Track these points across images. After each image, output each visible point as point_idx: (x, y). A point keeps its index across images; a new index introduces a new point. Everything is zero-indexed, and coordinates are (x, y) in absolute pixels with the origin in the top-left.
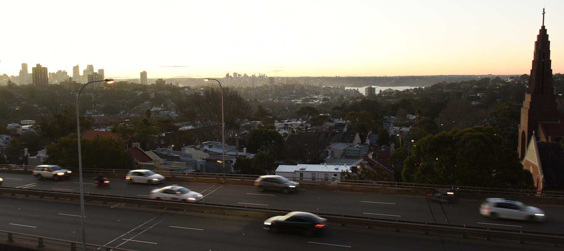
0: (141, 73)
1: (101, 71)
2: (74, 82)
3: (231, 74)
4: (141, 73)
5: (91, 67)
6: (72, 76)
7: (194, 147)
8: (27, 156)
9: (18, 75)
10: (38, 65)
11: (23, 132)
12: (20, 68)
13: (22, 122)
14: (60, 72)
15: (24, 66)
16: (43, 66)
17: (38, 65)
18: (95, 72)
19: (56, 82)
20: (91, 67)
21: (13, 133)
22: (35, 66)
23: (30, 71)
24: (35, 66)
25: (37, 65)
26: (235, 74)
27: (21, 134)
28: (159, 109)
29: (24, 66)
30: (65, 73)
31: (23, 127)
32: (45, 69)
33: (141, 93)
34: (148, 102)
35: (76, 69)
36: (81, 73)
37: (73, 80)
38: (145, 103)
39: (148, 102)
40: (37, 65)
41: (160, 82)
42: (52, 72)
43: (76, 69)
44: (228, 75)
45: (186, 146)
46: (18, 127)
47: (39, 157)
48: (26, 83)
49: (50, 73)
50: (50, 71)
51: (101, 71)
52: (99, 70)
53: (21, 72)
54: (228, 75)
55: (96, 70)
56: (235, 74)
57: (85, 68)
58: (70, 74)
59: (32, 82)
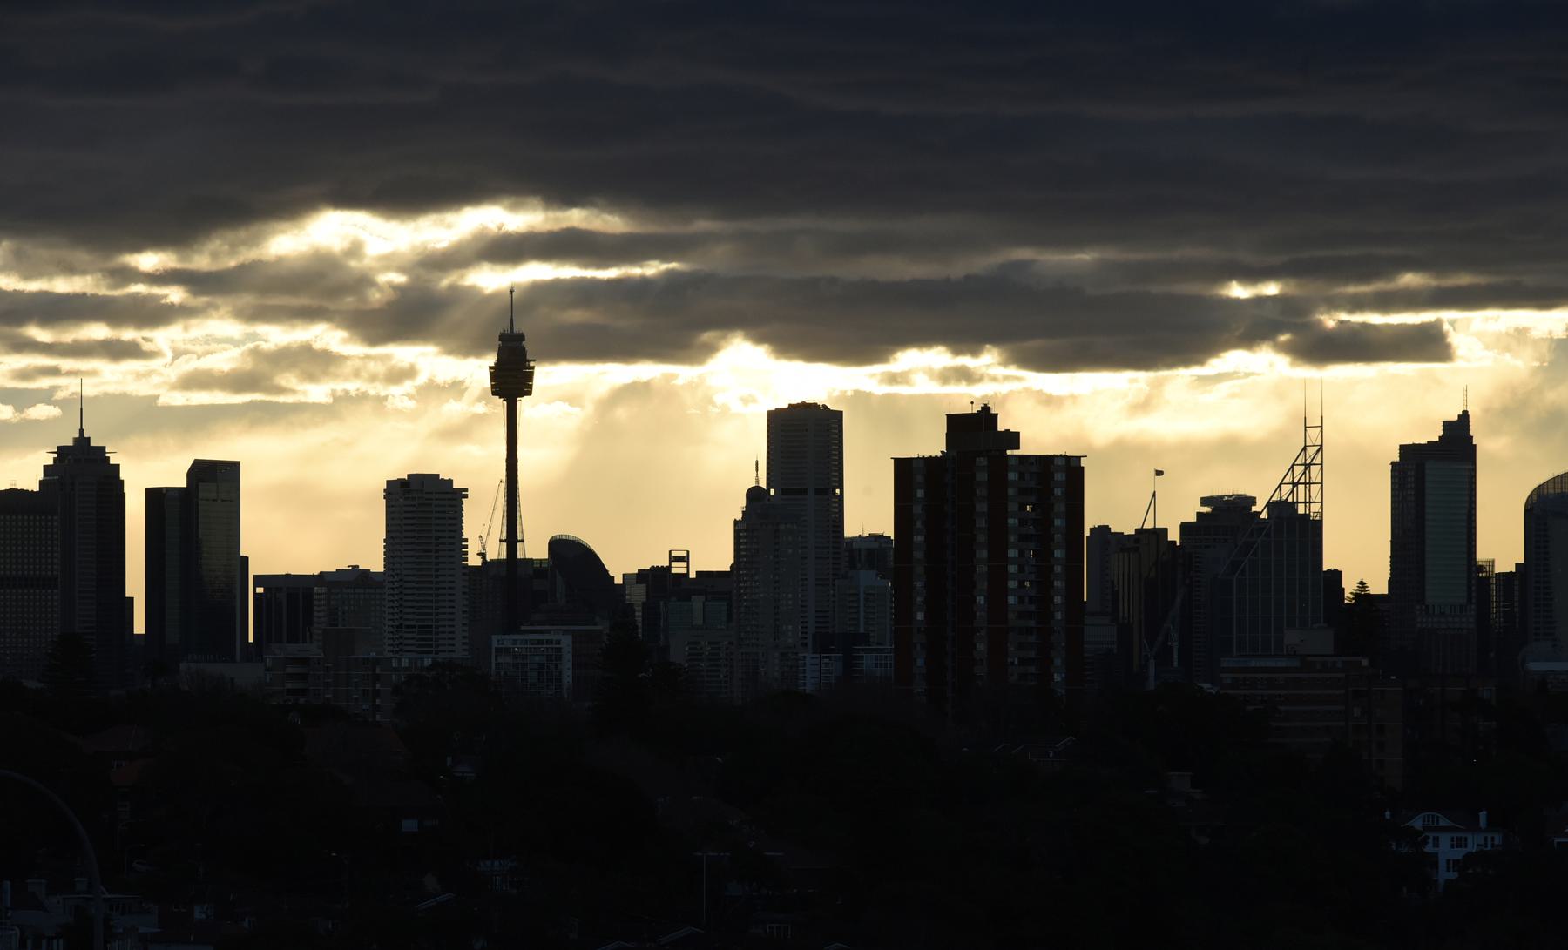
6: (1379, 585)
14: (1226, 516)
23: (868, 509)
25: (956, 423)
30: (1294, 530)
36: (1500, 542)
40: (956, 423)
42: (1125, 525)
49: (1102, 532)
50: (1110, 507)
53: (761, 519)
58: (1359, 552)
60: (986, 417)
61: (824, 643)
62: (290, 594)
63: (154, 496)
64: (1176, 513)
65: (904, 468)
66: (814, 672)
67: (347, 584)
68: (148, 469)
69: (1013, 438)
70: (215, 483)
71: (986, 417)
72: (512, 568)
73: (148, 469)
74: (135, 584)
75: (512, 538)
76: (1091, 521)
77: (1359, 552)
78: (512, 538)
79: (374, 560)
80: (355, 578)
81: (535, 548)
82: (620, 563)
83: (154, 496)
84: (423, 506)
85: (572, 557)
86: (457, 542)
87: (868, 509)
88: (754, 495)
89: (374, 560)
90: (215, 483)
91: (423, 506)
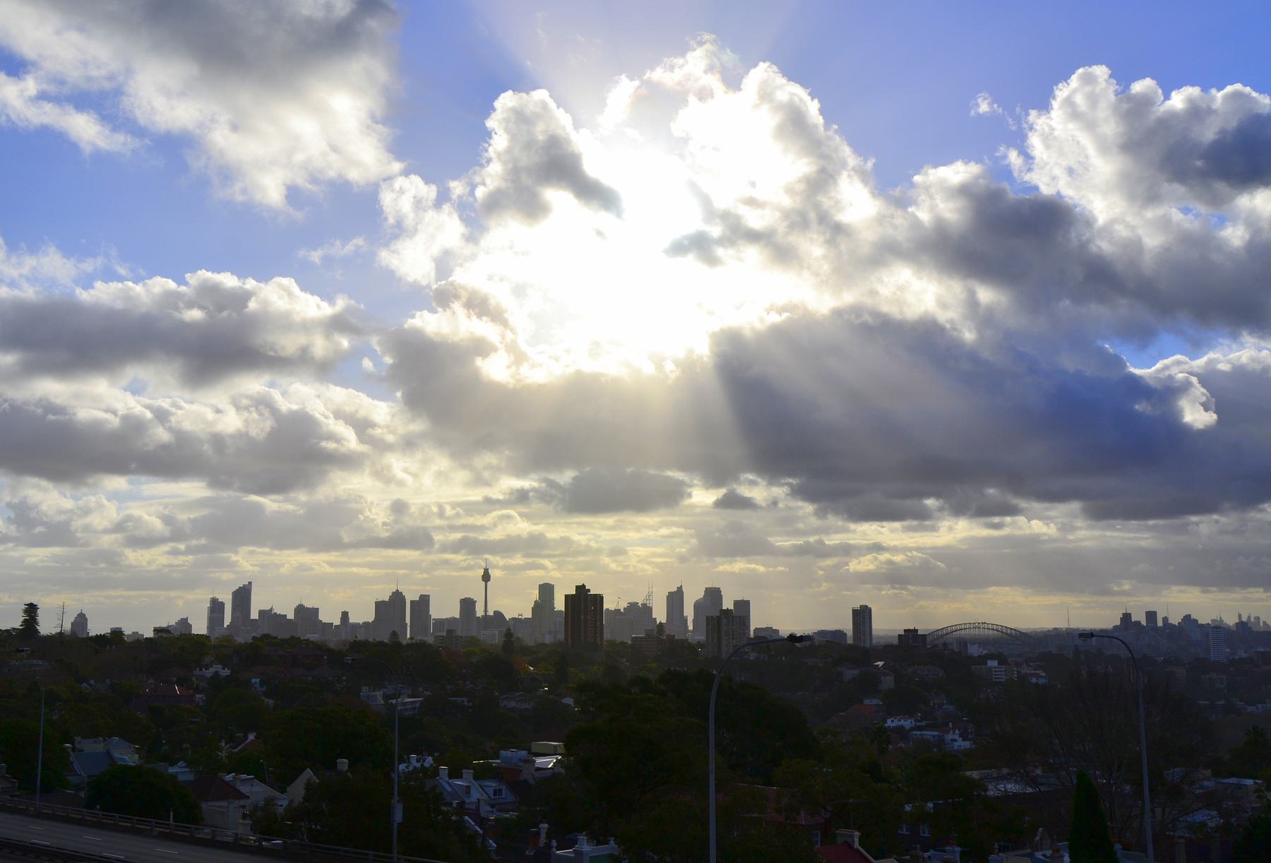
0: (855, 612)
1: (743, 606)
2: (671, 638)
3: (1139, 617)
4: (855, 612)
5: (713, 594)
6: (664, 621)
7: (1031, 856)
8: (548, 846)
10: (581, 589)
11: (537, 775)
12: (535, 595)
14: (633, 606)
15: (546, 590)
17: (581, 589)
19: (626, 637)
20: (713, 594)
21: (511, 777)
23: (560, 605)
25: (577, 587)
26: (1151, 616)
27: (532, 782)
28: (907, 723)
29: (546, 590)
31: (540, 761)
32: (599, 599)
33: (856, 672)
34: (875, 702)
35: (675, 599)
37: (667, 632)
38: (867, 702)
39: (875, 702)
40: (577, 587)
43: (675, 599)
44: (1126, 617)
45: (1003, 849)
46: (525, 761)
47: (579, 854)
48: (548, 640)
50: (608, 605)
51: (743, 606)
52: (737, 603)
53: (537, 608)
54: (1126, 617)
55: (728, 604)
56: (1151, 616)
58: (660, 615)
59: (561, 637)
60: (584, 586)
61: (550, 633)
62: (440, 622)
63: (412, 602)
64: (622, 606)
67: (452, 620)
68: (411, 595)
71: (584, 586)
72: (486, 616)
73: (411, 595)
74: (408, 620)
75: (486, 611)
76: (606, 606)
77: (660, 615)
78: (486, 611)
79: (458, 616)
81: (491, 613)
83: (412, 602)
84: (467, 604)
85: (498, 615)
89: (458, 616)
91: (467, 604)
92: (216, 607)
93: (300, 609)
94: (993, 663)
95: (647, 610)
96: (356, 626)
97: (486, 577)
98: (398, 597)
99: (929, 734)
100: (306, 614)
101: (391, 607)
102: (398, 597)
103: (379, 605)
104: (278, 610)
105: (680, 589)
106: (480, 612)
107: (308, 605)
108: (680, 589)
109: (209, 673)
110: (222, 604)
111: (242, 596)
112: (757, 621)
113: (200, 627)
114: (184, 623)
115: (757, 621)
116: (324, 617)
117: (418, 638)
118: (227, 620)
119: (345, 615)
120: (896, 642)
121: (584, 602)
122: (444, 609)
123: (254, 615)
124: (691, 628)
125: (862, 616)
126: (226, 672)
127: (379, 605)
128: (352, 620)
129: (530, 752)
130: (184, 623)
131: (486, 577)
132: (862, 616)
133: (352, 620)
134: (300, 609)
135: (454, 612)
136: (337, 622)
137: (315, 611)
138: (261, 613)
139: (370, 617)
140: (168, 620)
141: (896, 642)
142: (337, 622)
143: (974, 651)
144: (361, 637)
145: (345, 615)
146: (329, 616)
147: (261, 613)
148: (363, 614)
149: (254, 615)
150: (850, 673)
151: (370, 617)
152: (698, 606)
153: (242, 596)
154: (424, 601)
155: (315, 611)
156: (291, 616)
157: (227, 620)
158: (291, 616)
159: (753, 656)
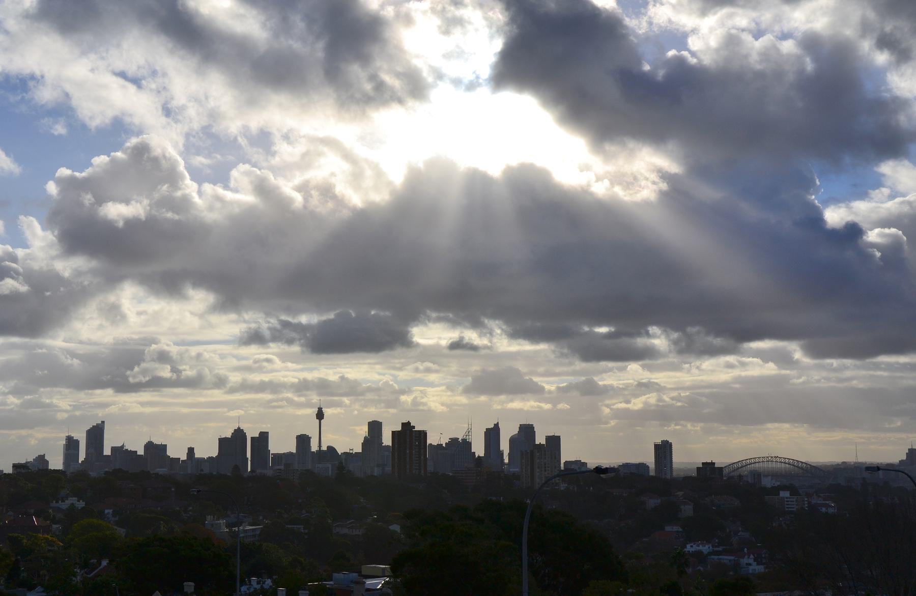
0: (657, 447)
1: (554, 442)
4: (657, 447)
5: (527, 431)
6: (482, 455)
9: (358, 449)
10: (407, 426)
12: (363, 431)
13: (367, 568)
14: (453, 442)
16: (418, 428)
17: (407, 426)
18: (537, 442)
20: (527, 431)
22: (399, 428)
23: (387, 440)
24: (399, 428)
28: (705, 548)
29: (375, 427)
31: (369, 582)
32: (423, 435)
34: (676, 528)
35: (492, 435)
38: (668, 528)
39: (676, 528)
41: (709, 472)
43: (492, 435)
46: (357, 583)
49: (431, 445)
50: (432, 440)
51: (554, 442)
52: (549, 439)
53: (366, 443)
57: (515, 431)
58: (479, 449)
59: (389, 469)
60: (409, 423)
62: (278, 457)
64: (444, 441)
65: (393, 433)
66: (377, 472)
68: (252, 432)
69: (414, 427)
70: (264, 436)
71: (409, 423)
72: (320, 451)
73: (252, 432)
75: (320, 446)
76: (429, 442)
77: (479, 449)
78: (320, 446)
80: (291, 454)
81: (324, 448)
82: (340, 451)
84: (303, 441)
85: (331, 449)
86: (310, 447)
87: (387, 440)
88: (365, 438)
90: (264, 436)
92: (71, 444)
93: (149, 446)
94: (785, 494)
95: (466, 444)
96: (201, 460)
97: (320, 415)
98: (239, 434)
99: (727, 559)
100: (155, 450)
101: (233, 444)
102: (239, 434)
103: (222, 442)
104: (130, 447)
105: (497, 425)
106: (314, 448)
107: (157, 441)
108: (497, 425)
109: (65, 505)
110: (77, 442)
111: (96, 434)
112: (567, 455)
113: (56, 462)
114: (41, 459)
115: (567, 455)
116: (171, 453)
117: (259, 471)
118: (82, 457)
119: (191, 451)
120: (694, 474)
121: (409, 437)
122: (282, 444)
123: (107, 451)
124: (506, 461)
125: (663, 450)
126: (81, 504)
127: (222, 442)
128: (198, 455)
129: (360, 575)
130: (41, 459)
131: (320, 415)
132: (663, 450)
133: (198, 455)
134: (149, 446)
135: (292, 447)
136: (184, 457)
137: (164, 447)
138: (114, 449)
139: (214, 452)
140: (26, 456)
141: (694, 474)
142: (184, 457)
143: (767, 482)
144: (206, 470)
145: (191, 451)
146: (177, 452)
147: (114, 449)
148: (208, 450)
149: (107, 451)
150: (652, 502)
151: (214, 452)
152: (513, 441)
153: (96, 434)
154: (262, 439)
155: (164, 447)
156: (141, 452)
157: (82, 457)
158: (141, 452)
159: (563, 486)
